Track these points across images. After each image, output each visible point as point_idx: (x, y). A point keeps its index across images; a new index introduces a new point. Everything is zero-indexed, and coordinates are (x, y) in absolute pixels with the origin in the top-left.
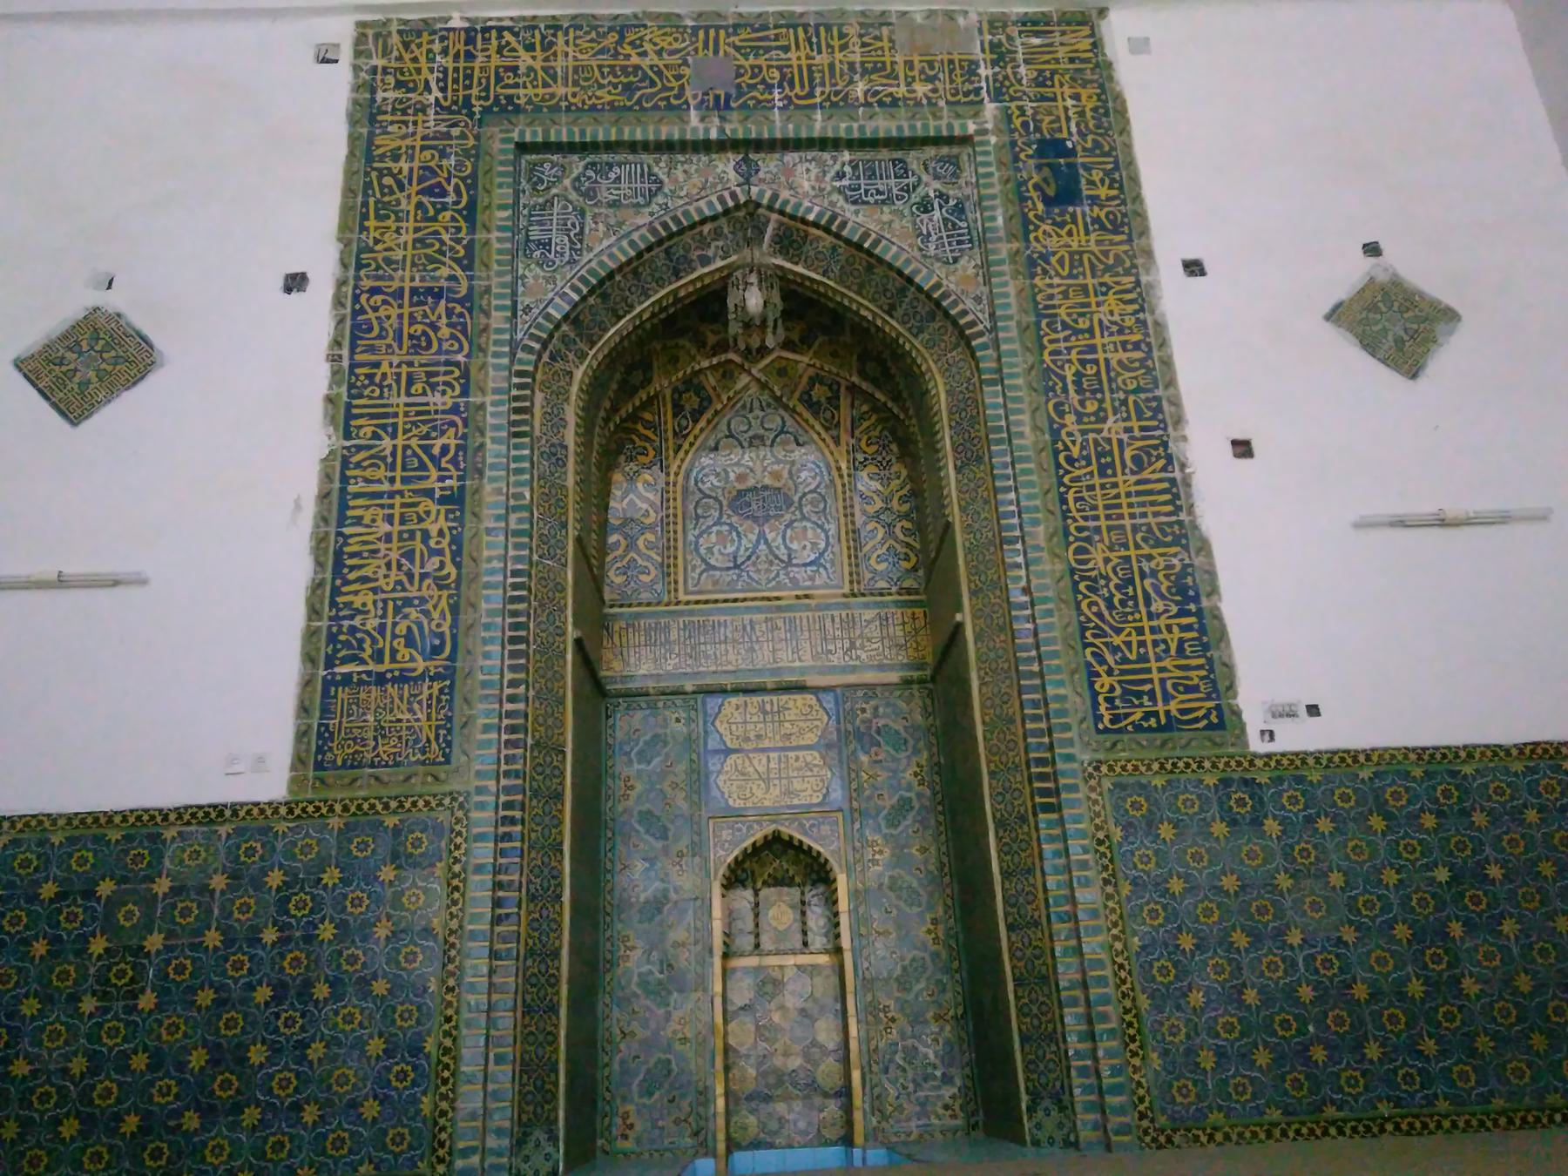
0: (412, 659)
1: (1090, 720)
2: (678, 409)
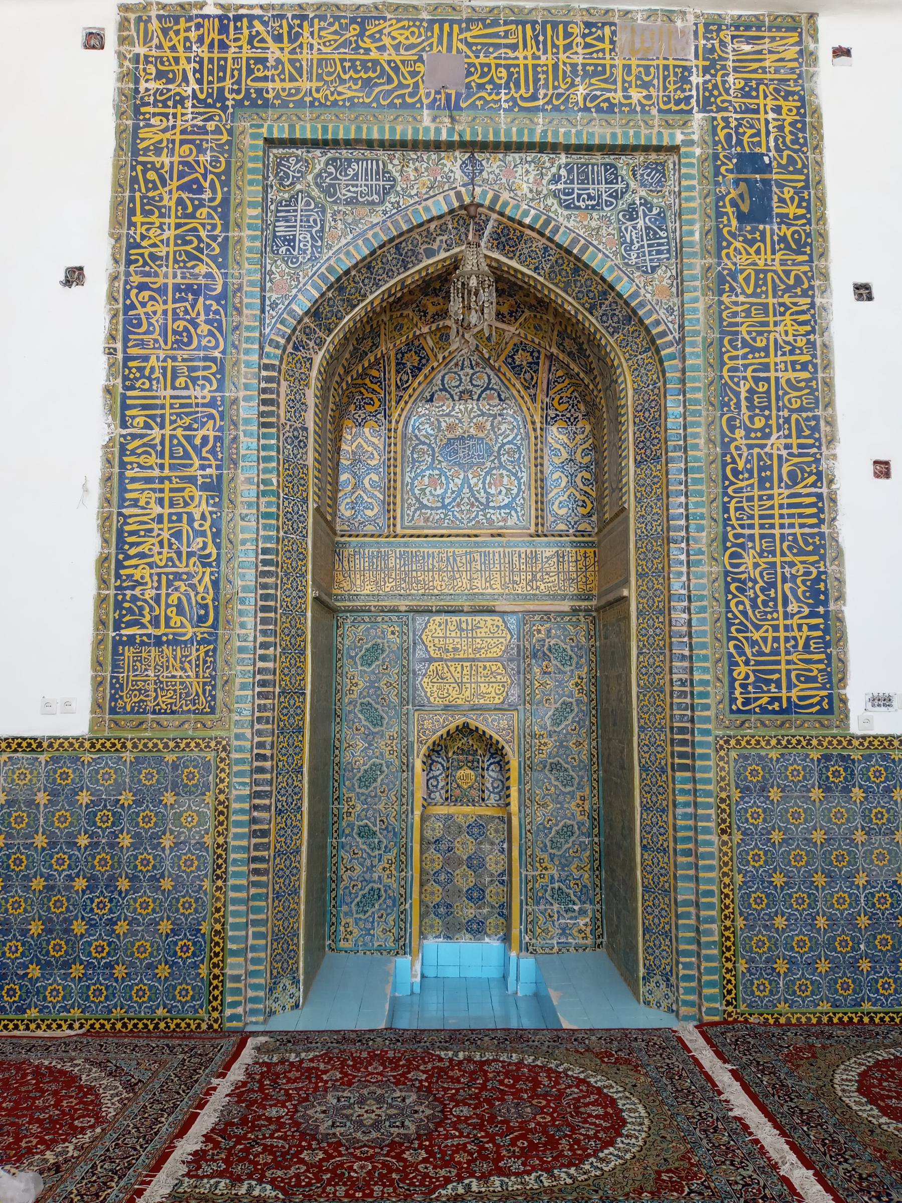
0: (182, 626)
1: (727, 701)
2: (400, 366)
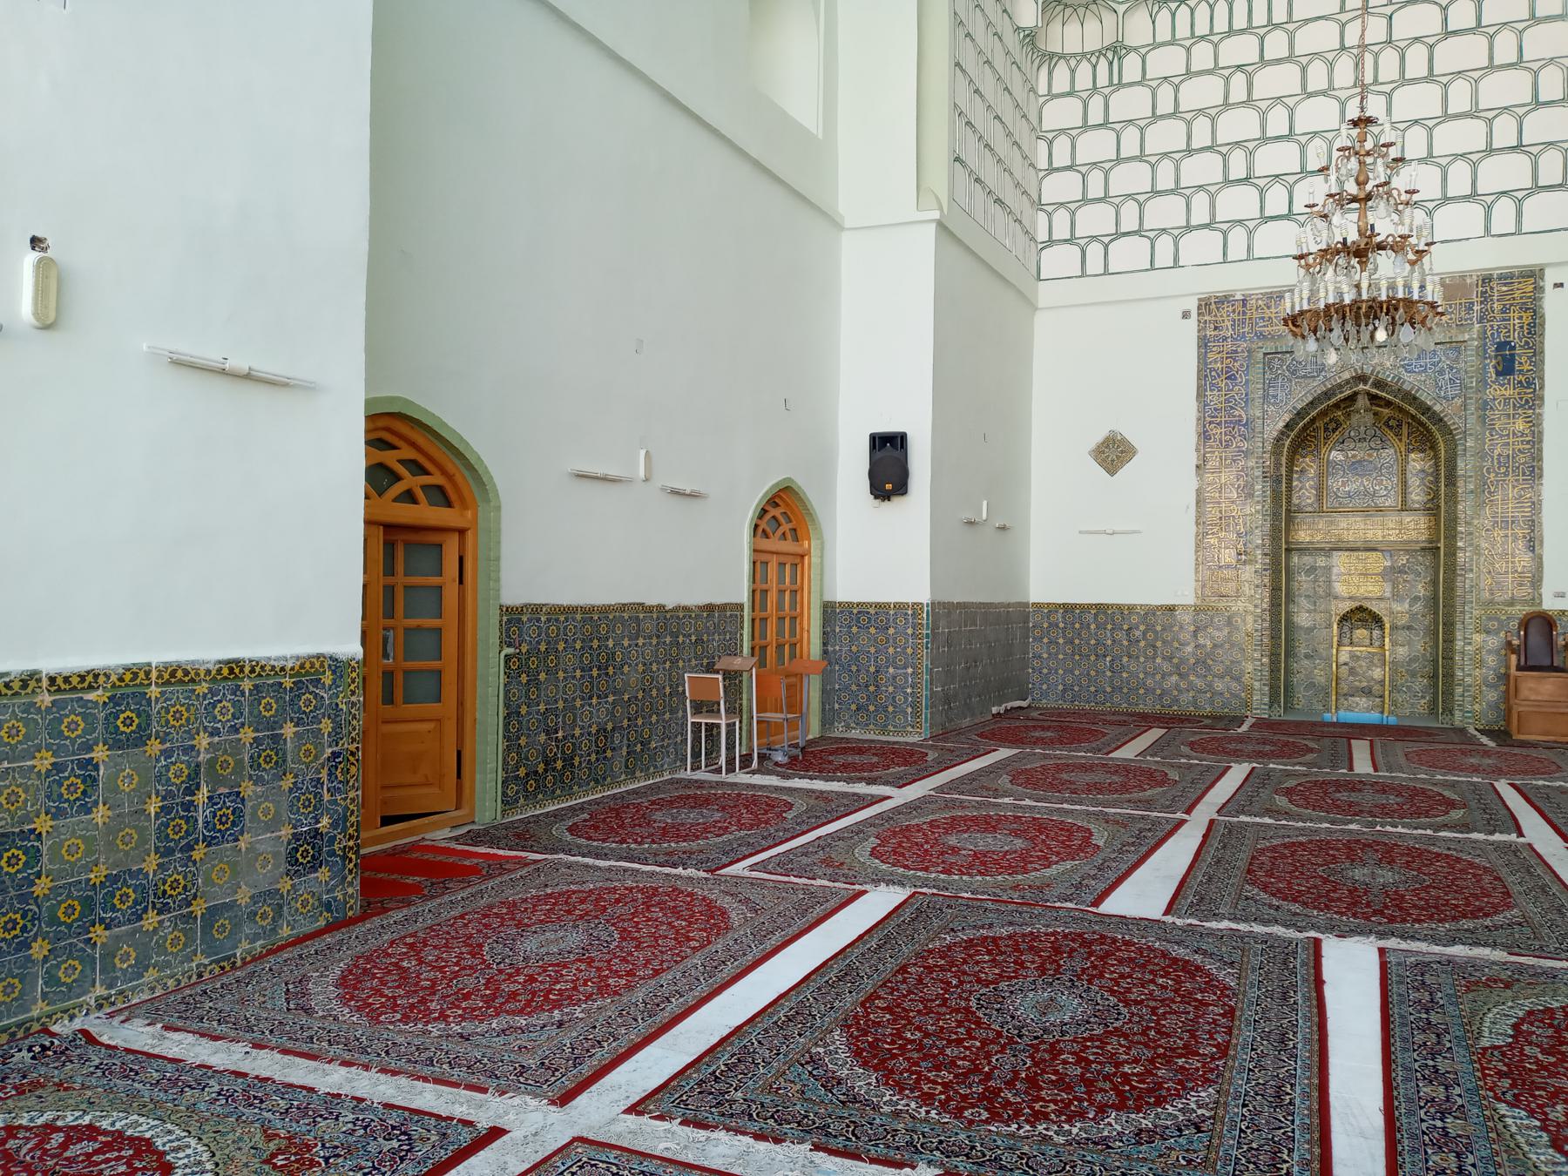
2: (1326, 429)
